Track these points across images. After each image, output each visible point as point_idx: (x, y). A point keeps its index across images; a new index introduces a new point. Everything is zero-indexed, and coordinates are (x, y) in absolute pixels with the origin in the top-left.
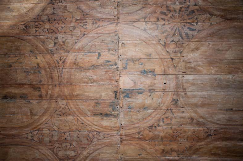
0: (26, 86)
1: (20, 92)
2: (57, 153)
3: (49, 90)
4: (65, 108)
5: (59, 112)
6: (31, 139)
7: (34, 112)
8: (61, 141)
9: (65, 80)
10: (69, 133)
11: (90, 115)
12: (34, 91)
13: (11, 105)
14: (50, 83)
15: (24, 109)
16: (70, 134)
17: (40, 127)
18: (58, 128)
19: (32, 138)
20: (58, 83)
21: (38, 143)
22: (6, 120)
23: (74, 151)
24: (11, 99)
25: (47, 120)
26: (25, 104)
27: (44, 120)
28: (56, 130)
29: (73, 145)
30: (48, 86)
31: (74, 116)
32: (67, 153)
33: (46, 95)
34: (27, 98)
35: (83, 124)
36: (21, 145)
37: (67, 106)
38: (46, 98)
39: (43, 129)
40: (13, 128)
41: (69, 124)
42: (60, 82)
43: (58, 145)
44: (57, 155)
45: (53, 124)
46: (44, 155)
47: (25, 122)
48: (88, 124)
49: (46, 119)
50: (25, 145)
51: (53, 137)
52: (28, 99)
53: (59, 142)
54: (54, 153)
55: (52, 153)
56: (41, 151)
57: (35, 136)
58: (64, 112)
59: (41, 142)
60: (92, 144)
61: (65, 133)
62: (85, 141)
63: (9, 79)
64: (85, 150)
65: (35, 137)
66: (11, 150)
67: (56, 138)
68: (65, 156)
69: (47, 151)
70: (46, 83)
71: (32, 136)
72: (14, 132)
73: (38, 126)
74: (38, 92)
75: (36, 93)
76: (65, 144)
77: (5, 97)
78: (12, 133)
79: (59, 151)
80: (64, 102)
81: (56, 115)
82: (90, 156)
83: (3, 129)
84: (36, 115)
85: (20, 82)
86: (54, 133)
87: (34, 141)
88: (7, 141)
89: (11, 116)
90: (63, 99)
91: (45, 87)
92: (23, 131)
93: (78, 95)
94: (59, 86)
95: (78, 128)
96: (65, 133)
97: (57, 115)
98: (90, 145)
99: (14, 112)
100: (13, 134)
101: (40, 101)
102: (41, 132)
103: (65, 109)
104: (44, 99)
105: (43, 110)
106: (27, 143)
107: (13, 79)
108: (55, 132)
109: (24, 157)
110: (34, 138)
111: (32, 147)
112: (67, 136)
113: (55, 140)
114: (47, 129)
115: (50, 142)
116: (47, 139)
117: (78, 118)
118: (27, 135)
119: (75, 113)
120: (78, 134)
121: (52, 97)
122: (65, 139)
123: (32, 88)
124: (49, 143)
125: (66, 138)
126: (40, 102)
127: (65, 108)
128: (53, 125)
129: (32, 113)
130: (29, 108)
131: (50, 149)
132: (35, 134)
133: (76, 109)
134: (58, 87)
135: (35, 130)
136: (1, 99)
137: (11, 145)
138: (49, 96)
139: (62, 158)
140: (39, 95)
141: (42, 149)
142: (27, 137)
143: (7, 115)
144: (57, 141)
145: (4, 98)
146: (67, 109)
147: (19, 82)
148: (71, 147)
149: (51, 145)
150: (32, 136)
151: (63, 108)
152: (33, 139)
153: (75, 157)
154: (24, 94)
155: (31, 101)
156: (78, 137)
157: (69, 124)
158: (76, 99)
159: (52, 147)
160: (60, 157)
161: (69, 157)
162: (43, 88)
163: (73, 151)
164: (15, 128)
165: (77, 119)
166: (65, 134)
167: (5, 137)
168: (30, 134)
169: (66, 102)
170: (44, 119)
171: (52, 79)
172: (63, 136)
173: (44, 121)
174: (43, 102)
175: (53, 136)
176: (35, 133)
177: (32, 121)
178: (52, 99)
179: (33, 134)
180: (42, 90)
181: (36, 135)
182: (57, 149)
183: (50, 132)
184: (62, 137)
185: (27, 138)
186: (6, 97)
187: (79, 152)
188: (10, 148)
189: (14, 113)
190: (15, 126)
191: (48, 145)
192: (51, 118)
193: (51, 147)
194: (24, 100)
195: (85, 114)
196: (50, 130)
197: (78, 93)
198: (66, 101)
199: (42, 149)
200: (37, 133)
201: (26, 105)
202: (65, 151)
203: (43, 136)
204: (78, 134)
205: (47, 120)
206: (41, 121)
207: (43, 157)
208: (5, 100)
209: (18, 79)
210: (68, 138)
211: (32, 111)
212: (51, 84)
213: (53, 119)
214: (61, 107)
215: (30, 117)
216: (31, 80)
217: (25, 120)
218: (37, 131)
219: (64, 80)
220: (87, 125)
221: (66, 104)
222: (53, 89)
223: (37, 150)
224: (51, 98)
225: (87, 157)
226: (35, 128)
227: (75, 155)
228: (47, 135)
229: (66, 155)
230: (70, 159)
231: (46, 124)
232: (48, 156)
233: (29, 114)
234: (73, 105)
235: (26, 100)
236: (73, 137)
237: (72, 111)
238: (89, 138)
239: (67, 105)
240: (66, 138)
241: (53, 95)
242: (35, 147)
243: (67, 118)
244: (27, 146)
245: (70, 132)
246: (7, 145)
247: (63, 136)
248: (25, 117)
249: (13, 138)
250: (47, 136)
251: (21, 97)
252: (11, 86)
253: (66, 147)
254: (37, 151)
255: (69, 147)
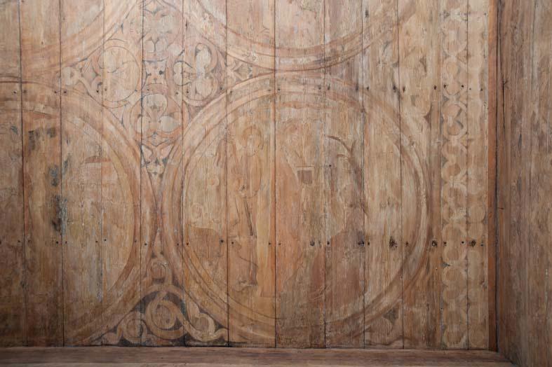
0: (27, 169)
1: (42, 184)
2: (203, 100)
3: (36, 109)
4: (81, 69)
5: (90, 85)
6: (163, 165)
7: (91, 151)
8: (168, 86)
9: (11, 65)
10: (146, 62)
11: (99, 6)
12: (39, 148)
13: (75, 210)
14: (18, 106)
15: (85, 179)
16: (150, 62)
17: (131, 140)
18: (135, 93)
19: (161, 162)
20: (17, 84)
21: (175, 148)
22: (115, 227)
23: (197, 52)
24: (61, 210)
25: (113, 119)
26: (71, 172)
27: (112, 128)
28: (140, 97)
29: (180, 55)
30: (26, 111)
31: (102, 49)
32: (203, 71)
33: (49, 117)
34: (56, 166)
35: (122, 26)
36: (181, 193)
37: (77, 64)
38: (58, 119)
39: (137, 133)
40: (137, 210)
41: (123, 63)
42: (16, 80)
43: (180, 94)
44: (207, 100)
45: (122, 103)
46: (207, 133)
47: (118, 179)
48: (124, 13)
49: (111, 122)
50: (182, 183)
51: (157, 105)
52: (59, 165)
53: (172, 92)
54: (203, 107)
55: (202, 111)
56: (196, 143)
57: (156, 154)
58: (91, 74)
59: (174, 141)
60: (177, 5)
61: (147, 75)
62: (169, 24)
63: (10, 210)
64: (194, 24)
65: (158, 154)
66: (193, 220)
67: (161, 100)
68: (211, 78)
69: (198, 127)
70: (19, 117)
71: (157, 162)
72: (146, 209)
73: (129, 144)
74: (41, 139)
75: (44, 143)
76: (178, 76)
77: (56, 224)
78: (148, 213)
79: (196, 92)
80: (67, 71)
81: (100, 95)
82: (209, 10)
83: (137, 238)
84: (100, 148)
85: (17, 182)
86: (148, 102)
87: (171, 157)
88: (169, 229)
89: (105, 214)
90: (58, 74)
91: (27, 118)
92: (144, 185)
93: (49, 35)
94: (26, 82)
95: (134, 38)
96: (147, 75)
97: (100, 92)
98: (181, 10)
99: (92, 203)
100: (150, 213)
101: (63, 135)
102: (145, 137)
103: (83, 72)
104: (58, 125)
105: (89, 130)
106: (174, 178)
107: (9, 199)
108: (145, 99)
109: (214, 187)
110: (162, 157)
111: (187, 165)
112: (156, 68)
113: (166, 100)
114: (136, 121)
115: (171, 115)
116: (165, 124)
117: (108, 36)
118: (153, 175)
119: (95, 45)
120: (151, 39)
121: (53, 104)
122: (163, 75)
123: (32, 154)
124: (174, 117)
125: (161, 73)
126: (67, 134)
127: (81, 69)
128: (125, 105)
129: (95, 157)
130: (81, 164)
131: (191, 116)
132: (150, 152)
133: (84, 43)
134: (28, 84)
135: (139, 154)
136: (61, 234)
137: (180, 219)
138: (51, 111)
139: (216, 87)
140: (49, 136)
141: (193, 139)
142: (157, 175)
143: (103, 223)
144: (168, 95)
145: (58, 228)
146: (83, 66)
147: (15, 184)
148: (184, 59)
149: (180, 114)
150: (157, 162)
151: (82, 76)
152: (165, 161)
153: (213, 51)
154: (47, 176)
155: (65, 159)
156: (158, 40)
157: (123, 63)
158: (58, 41)
159: (186, 110)
160: (214, 92)
161: (214, 64)
162: (31, 124)
163: (196, 55)
164: (134, 206)
165: (109, 39)
166: (150, 75)
167: (158, 234)
168: (151, 166)
169: (66, 67)
170: (109, 127)
171: (7, 99)
172: (155, 79)
173: (116, 128)
174: (67, 126)
175: (155, 107)
176: (147, 153)
177: (114, 158)
178: (58, 103)
179: (149, 160)
180: (35, 127)
181: (152, 151)
182: (192, 96)
183: (144, 113)
184: (158, 82)
185: (161, 176)
186: (56, 222)
187: (198, 39)
188: (189, 224)
189: (97, 206)
190: (130, 206)
191: (180, 120)
192: (107, 108)
193: (186, 115)
194: (63, 176)
195: (95, 19)
196: (140, 112)
197: (42, 35)
198: (63, 66)
199: (193, 139)
200: (148, 148)
201: (75, 172)
202: (196, 78)
203: (154, 133)
204: (151, 39)
205: (113, 119)
206: (117, 135)
207: (212, 136)
208: (64, 224)
209: (9, 187)
210: (161, 66)
211: (90, 158)
212: (22, 104)
213: (110, 105)
214: (79, 81)
215: (106, 164)
216: (9, 154)
217: (114, 178)
218: (143, 148)
219: (10, 67)
220: (125, 15)
221: (71, 66)
222: (33, 99)
223: (194, 151)
224: (58, 106)
225: (212, 19)
226: (135, 153)
227: (206, 51)
228: (152, 123)
229: (207, 74)
230: (217, 64)
231: (124, 123)
232: (212, 124)
233: (98, 165)
234: (72, 48)
235: (63, 171)
236: (157, 54)
237: (88, 53)
238: (160, 12)
239: (73, 66)
240: (161, 73)
241: (49, 98)
242: (187, 157)
243: (108, 67)
244: (183, 177)
245: (143, 61)
246: (182, 232)
247: (155, 79)
248: (106, 179)
249: (162, 214)
250: (155, 121)
251: (55, 184)
252: (28, 207)
253: (185, 74)
254: (197, 152)
255: (185, 66)
